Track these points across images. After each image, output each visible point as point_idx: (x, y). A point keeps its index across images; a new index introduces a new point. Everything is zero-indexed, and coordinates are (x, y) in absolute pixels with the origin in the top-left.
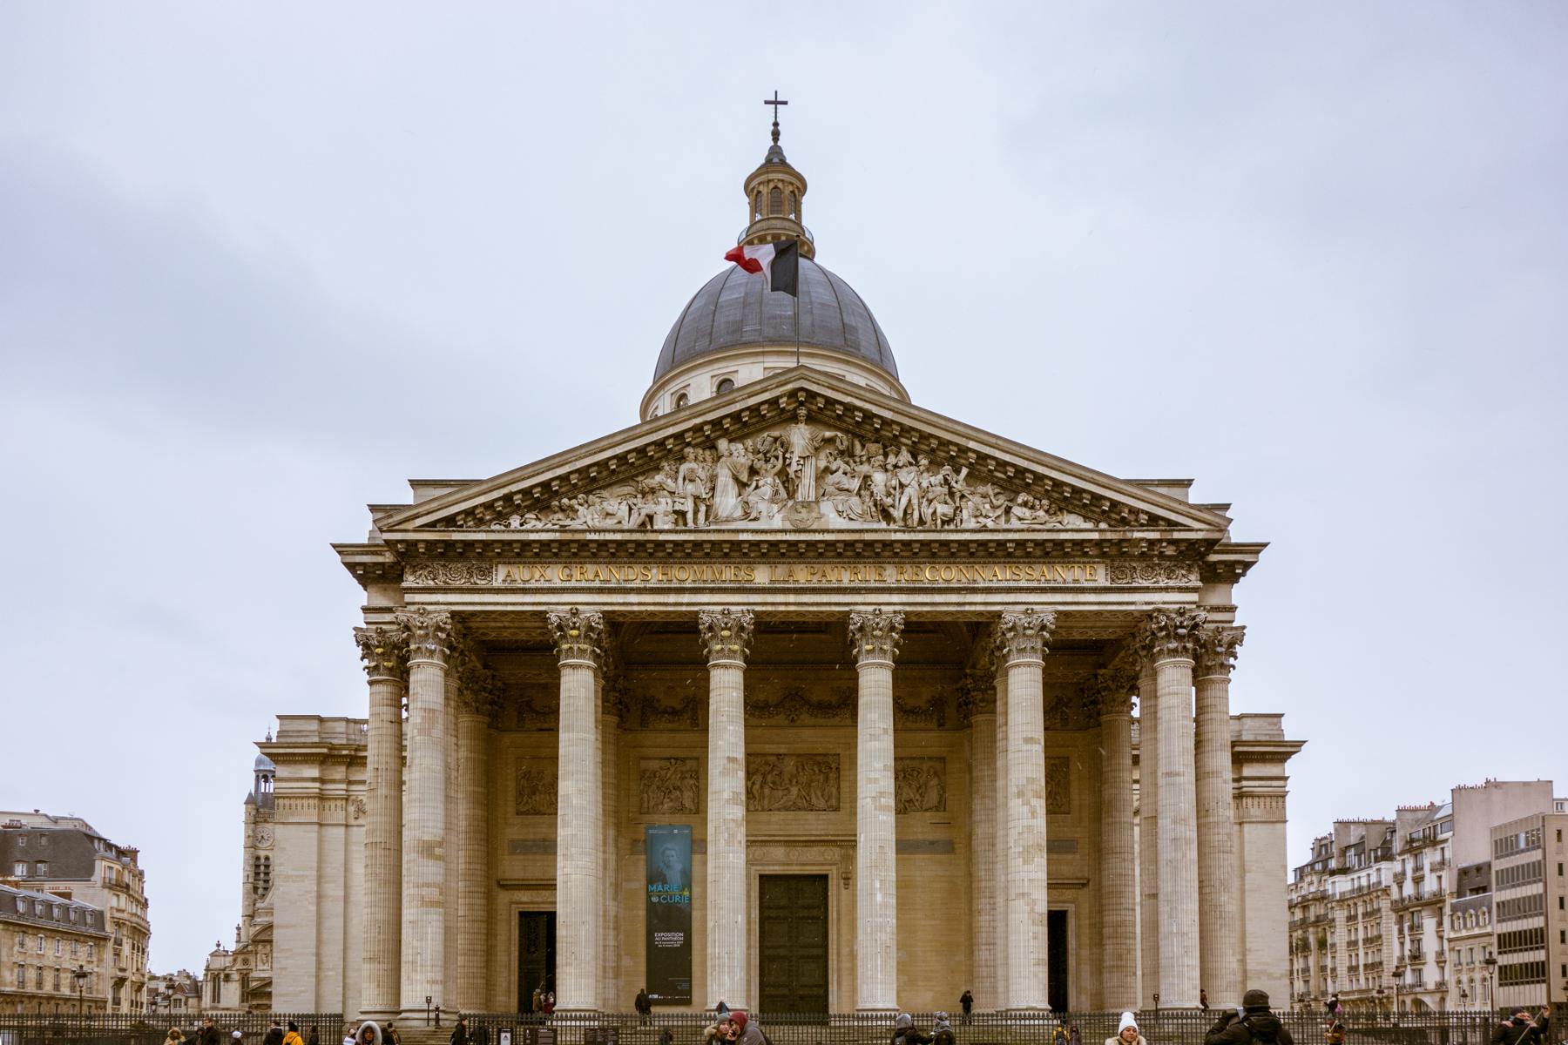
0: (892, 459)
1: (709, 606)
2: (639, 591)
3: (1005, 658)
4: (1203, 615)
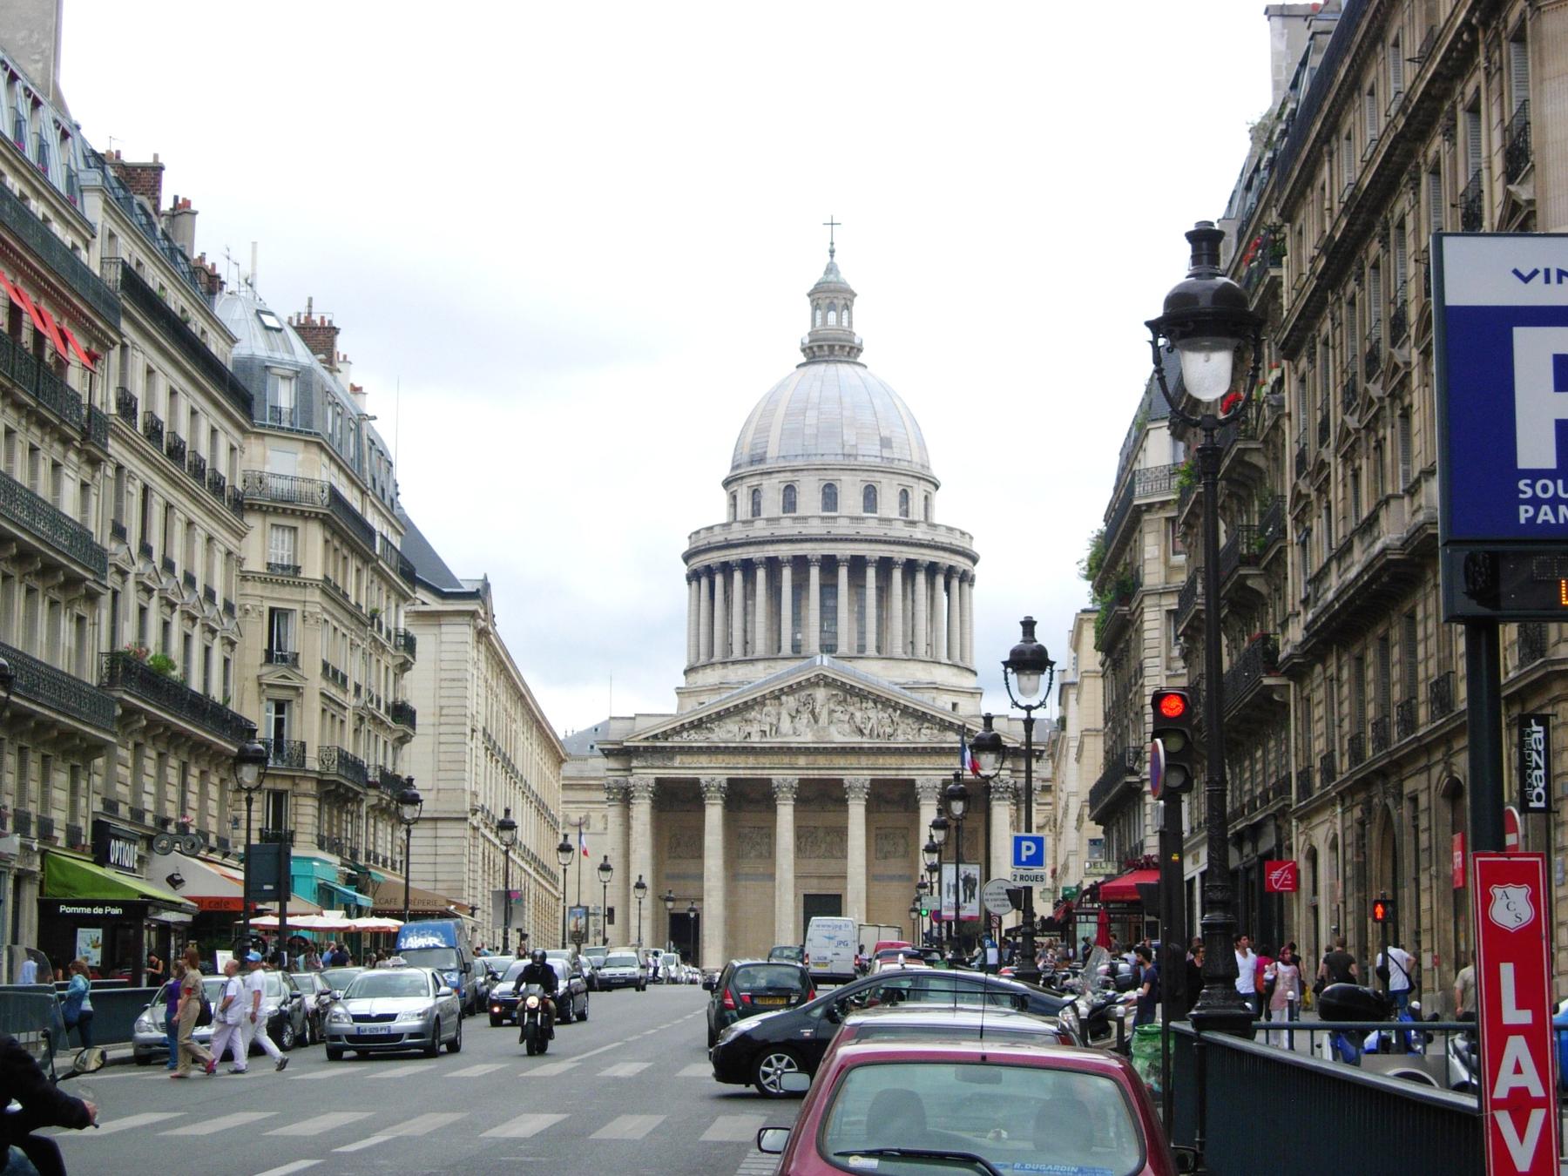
1: (777, 776)
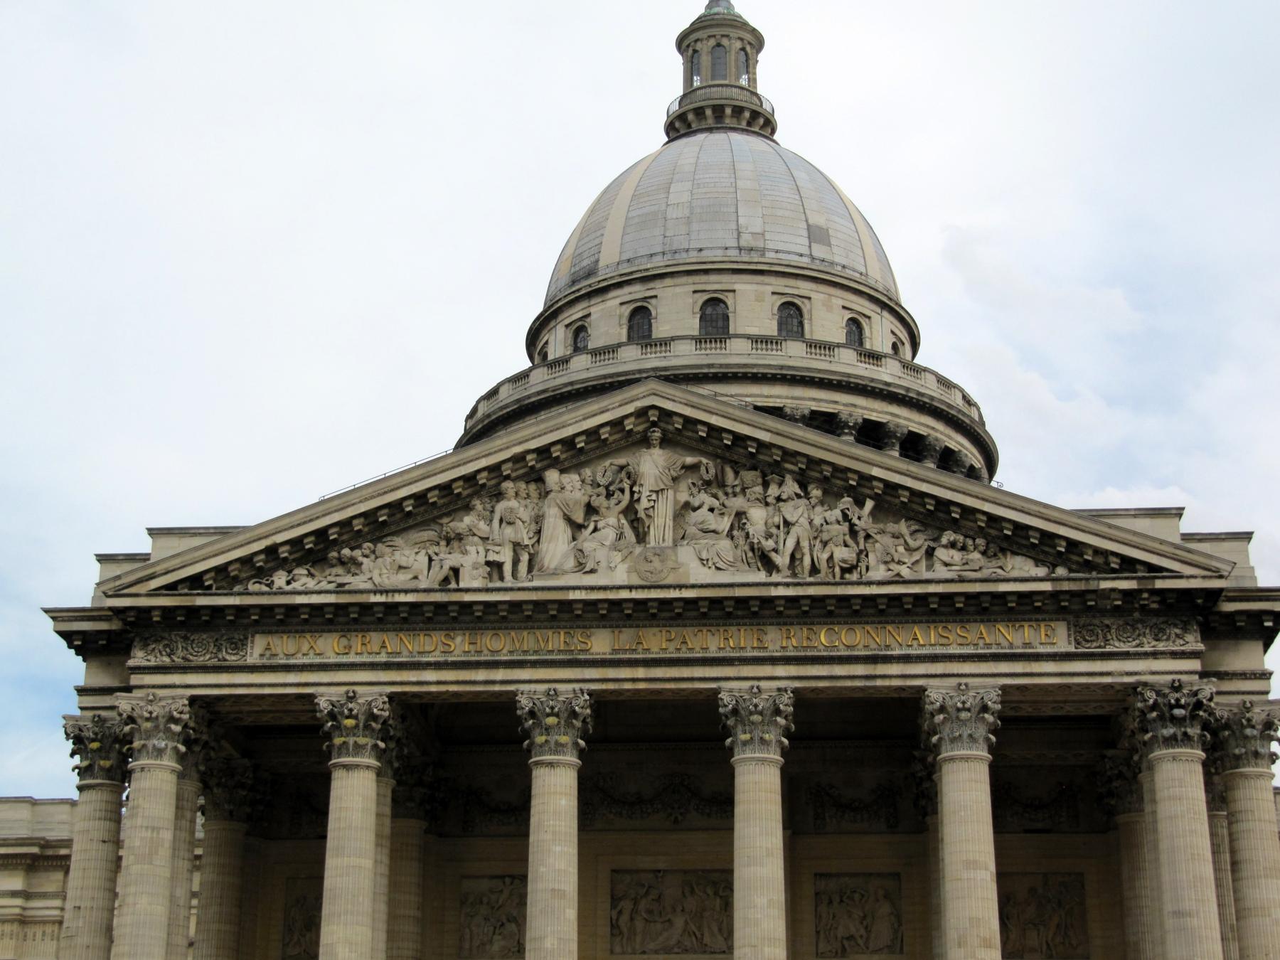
0: (773, 491)
1: (530, 686)
2: (438, 666)
3: (936, 749)
4: (1208, 688)
